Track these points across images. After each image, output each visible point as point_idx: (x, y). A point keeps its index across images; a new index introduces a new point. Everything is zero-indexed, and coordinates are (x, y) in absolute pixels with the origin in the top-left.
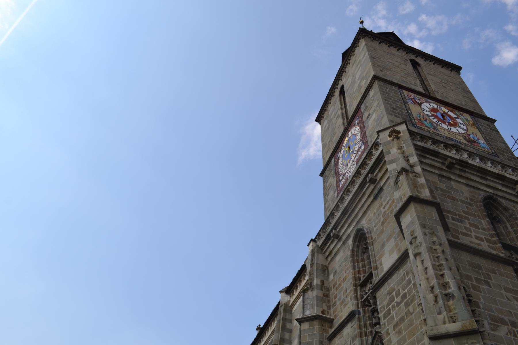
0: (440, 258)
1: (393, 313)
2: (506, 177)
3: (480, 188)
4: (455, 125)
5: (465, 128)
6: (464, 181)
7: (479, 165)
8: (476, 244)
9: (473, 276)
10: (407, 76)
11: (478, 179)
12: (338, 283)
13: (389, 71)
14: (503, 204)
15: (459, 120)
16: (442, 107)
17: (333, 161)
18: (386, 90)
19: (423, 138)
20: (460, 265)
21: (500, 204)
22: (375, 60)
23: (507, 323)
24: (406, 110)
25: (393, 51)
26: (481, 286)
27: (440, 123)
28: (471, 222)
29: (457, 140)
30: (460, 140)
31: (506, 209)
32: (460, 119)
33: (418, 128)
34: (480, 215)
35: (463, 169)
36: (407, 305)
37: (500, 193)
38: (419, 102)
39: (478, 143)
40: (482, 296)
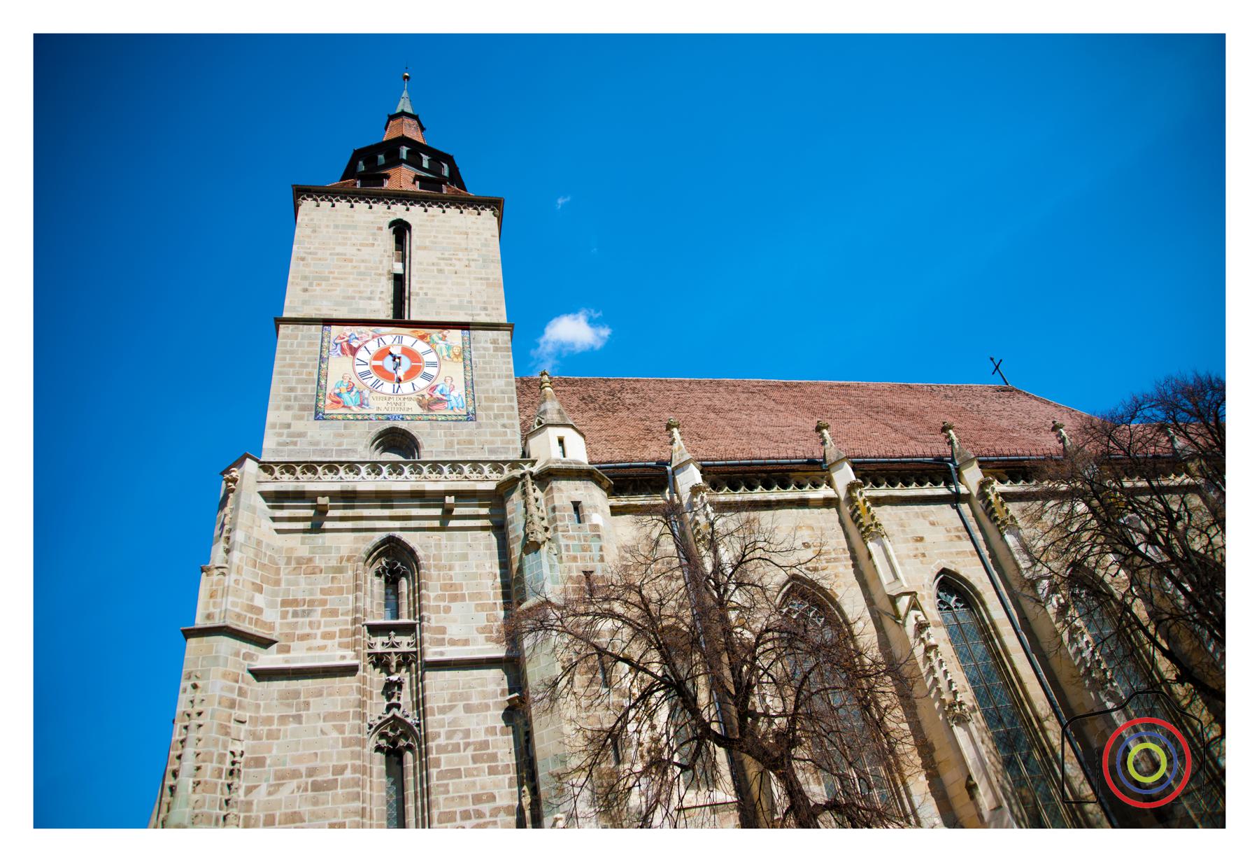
7: (377, 486)
18: (292, 344)
20: (262, 703)
22: (302, 262)
26: (282, 728)
28: (328, 607)
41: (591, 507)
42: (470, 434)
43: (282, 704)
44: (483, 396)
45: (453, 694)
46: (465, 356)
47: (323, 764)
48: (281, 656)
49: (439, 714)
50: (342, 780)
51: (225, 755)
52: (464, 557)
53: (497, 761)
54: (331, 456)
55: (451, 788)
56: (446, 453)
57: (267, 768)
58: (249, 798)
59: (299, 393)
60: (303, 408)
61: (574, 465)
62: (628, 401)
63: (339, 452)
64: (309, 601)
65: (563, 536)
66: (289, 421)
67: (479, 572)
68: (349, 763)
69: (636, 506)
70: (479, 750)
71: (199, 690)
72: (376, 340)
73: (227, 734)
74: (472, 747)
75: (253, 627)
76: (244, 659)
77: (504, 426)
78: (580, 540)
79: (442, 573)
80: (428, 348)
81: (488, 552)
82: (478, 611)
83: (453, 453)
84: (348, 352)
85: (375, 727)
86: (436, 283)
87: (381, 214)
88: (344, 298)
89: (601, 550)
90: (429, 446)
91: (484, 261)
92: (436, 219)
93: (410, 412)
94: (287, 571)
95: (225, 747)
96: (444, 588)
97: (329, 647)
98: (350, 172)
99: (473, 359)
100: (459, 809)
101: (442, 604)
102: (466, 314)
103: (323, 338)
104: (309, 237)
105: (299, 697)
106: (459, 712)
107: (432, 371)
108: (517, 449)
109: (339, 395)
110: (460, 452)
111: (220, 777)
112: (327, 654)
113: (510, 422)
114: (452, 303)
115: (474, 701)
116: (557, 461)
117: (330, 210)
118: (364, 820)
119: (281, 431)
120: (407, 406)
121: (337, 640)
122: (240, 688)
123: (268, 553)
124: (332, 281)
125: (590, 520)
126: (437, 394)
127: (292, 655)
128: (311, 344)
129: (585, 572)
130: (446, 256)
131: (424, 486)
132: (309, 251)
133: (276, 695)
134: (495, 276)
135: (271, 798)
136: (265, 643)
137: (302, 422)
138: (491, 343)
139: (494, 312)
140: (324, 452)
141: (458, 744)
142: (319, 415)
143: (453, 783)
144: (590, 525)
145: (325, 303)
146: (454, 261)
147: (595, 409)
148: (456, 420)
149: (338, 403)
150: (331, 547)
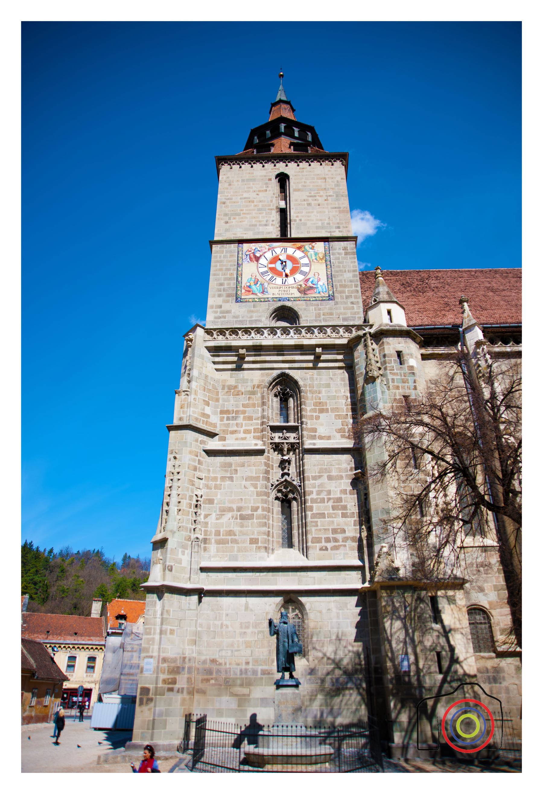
18: (220, 257)
20: (211, 469)
26: (223, 483)
28: (247, 415)
30: (292, 294)
33: (241, 302)
41: (408, 355)
42: (331, 309)
43: (222, 470)
44: (338, 284)
45: (321, 469)
46: (326, 259)
47: (246, 505)
48: (221, 443)
49: (312, 480)
50: (256, 515)
51: (193, 496)
52: (328, 386)
53: (347, 510)
54: (246, 324)
55: (319, 524)
56: (316, 321)
57: (215, 505)
58: (206, 520)
59: (226, 286)
60: (228, 296)
61: (397, 328)
62: (433, 285)
63: (251, 322)
64: (236, 411)
65: (390, 373)
66: (220, 303)
67: (337, 395)
68: (260, 505)
69: (438, 354)
70: (336, 503)
71: (177, 460)
72: (271, 251)
73: (193, 485)
74: (332, 501)
75: (205, 425)
76: (201, 444)
77: (352, 303)
78: (401, 375)
79: (314, 395)
80: (303, 255)
81: (343, 382)
83: (320, 321)
84: (254, 260)
85: (275, 486)
86: (307, 213)
87: (270, 170)
88: (250, 226)
89: (415, 382)
90: (305, 317)
91: (337, 196)
92: (304, 170)
93: (293, 296)
94: (223, 393)
95: (193, 492)
96: (315, 404)
97: (248, 438)
98: (249, 145)
99: (332, 261)
100: (324, 536)
101: (315, 414)
102: (326, 232)
103: (238, 252)
104: (227, 189)
105: (231, 467)
106: (324, 479)
107: (306, 269)
108: (360, 317)
109: (249, 287)
110: (325, 320)
111: (191, 508)
112: (248, 442)
113: (356, 300)
114: (317, 225)
115: (334, 473)
116: (387, 325)
117: (239, 170)
118: (269, 538)
119: (216, 310)
120: (291, 292)
121: (252, 434)
122: (199, 460)
123: (212, 383)
124: (242, 216)
125: (408, 363)
126: (309, 284)
127: (227, 442)
128: (231, 256)
129: (404, 396)
130: (312, 194)
131: (303, 341)
132: (229, 197)
133: (218, 465)
134: (344, 206)
135: (218, 521)
136: (212, 435)
137: (228, 304)
138: (343, 250)
139: (344, 230)
140: (241, 322)
141: (324, 498)
142: (238, 300)
143: (321, 521)
144: (408, 366)
145: (238, 230)
146: (317, 198)
147: (411, 291)
148: (322, 300)
149: (249, 291)
150: (248, 379)
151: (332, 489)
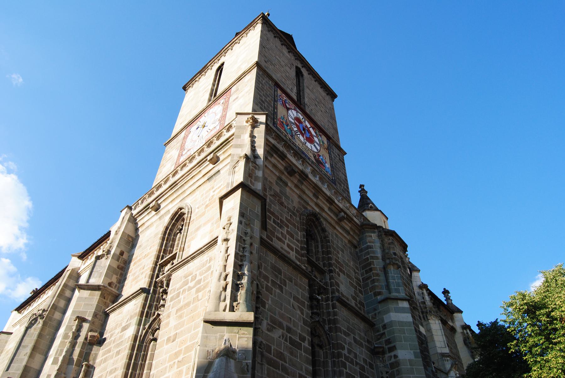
0: (245, 250)
1: (181, 297)
2: (334, 202)
3: (310, 204)
4: (311, 140)
5: (319, 148)
6: (298, 192)
7: (316, 182)
8: (286, 251)
9: (271, 278)
10: (287, 79)
11: (311, 195)
12: (138, 258)
13: (273, 66)
14: (323, 224)
15: (316, 139)
16: (306, 121)
17: (183, 134)
19: (278, 138)
20: (263, 264)
21: (320, 224)
22: (264, 49)
23: (284, 327)
24: (273, 107)
25: (284, 51)
26: (274, 289)
27: (299, 133)
28: (289, 230)
29: (308, 155)
30: (310, 156)
31: (324, 230)
32: (318, 138)
34: (300, 227)
35: (302, 181)
36: (198, 291)
37: (324, 214)
38: (288, 107)
39: (324, 166)
40: (271, 297)
47: (294, 328)
49: (344, 335)
52: (343, 251)
74: (358, 366)
82: (350, 285)
92: (312, 81)
93: (311, 158)
115: (357, 337)
128: (269, 88)
151: (358, 353)
